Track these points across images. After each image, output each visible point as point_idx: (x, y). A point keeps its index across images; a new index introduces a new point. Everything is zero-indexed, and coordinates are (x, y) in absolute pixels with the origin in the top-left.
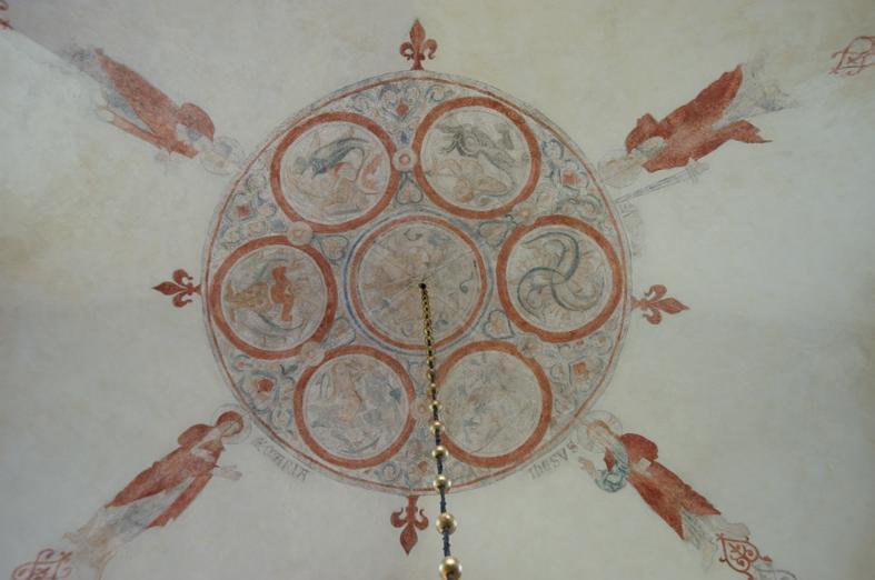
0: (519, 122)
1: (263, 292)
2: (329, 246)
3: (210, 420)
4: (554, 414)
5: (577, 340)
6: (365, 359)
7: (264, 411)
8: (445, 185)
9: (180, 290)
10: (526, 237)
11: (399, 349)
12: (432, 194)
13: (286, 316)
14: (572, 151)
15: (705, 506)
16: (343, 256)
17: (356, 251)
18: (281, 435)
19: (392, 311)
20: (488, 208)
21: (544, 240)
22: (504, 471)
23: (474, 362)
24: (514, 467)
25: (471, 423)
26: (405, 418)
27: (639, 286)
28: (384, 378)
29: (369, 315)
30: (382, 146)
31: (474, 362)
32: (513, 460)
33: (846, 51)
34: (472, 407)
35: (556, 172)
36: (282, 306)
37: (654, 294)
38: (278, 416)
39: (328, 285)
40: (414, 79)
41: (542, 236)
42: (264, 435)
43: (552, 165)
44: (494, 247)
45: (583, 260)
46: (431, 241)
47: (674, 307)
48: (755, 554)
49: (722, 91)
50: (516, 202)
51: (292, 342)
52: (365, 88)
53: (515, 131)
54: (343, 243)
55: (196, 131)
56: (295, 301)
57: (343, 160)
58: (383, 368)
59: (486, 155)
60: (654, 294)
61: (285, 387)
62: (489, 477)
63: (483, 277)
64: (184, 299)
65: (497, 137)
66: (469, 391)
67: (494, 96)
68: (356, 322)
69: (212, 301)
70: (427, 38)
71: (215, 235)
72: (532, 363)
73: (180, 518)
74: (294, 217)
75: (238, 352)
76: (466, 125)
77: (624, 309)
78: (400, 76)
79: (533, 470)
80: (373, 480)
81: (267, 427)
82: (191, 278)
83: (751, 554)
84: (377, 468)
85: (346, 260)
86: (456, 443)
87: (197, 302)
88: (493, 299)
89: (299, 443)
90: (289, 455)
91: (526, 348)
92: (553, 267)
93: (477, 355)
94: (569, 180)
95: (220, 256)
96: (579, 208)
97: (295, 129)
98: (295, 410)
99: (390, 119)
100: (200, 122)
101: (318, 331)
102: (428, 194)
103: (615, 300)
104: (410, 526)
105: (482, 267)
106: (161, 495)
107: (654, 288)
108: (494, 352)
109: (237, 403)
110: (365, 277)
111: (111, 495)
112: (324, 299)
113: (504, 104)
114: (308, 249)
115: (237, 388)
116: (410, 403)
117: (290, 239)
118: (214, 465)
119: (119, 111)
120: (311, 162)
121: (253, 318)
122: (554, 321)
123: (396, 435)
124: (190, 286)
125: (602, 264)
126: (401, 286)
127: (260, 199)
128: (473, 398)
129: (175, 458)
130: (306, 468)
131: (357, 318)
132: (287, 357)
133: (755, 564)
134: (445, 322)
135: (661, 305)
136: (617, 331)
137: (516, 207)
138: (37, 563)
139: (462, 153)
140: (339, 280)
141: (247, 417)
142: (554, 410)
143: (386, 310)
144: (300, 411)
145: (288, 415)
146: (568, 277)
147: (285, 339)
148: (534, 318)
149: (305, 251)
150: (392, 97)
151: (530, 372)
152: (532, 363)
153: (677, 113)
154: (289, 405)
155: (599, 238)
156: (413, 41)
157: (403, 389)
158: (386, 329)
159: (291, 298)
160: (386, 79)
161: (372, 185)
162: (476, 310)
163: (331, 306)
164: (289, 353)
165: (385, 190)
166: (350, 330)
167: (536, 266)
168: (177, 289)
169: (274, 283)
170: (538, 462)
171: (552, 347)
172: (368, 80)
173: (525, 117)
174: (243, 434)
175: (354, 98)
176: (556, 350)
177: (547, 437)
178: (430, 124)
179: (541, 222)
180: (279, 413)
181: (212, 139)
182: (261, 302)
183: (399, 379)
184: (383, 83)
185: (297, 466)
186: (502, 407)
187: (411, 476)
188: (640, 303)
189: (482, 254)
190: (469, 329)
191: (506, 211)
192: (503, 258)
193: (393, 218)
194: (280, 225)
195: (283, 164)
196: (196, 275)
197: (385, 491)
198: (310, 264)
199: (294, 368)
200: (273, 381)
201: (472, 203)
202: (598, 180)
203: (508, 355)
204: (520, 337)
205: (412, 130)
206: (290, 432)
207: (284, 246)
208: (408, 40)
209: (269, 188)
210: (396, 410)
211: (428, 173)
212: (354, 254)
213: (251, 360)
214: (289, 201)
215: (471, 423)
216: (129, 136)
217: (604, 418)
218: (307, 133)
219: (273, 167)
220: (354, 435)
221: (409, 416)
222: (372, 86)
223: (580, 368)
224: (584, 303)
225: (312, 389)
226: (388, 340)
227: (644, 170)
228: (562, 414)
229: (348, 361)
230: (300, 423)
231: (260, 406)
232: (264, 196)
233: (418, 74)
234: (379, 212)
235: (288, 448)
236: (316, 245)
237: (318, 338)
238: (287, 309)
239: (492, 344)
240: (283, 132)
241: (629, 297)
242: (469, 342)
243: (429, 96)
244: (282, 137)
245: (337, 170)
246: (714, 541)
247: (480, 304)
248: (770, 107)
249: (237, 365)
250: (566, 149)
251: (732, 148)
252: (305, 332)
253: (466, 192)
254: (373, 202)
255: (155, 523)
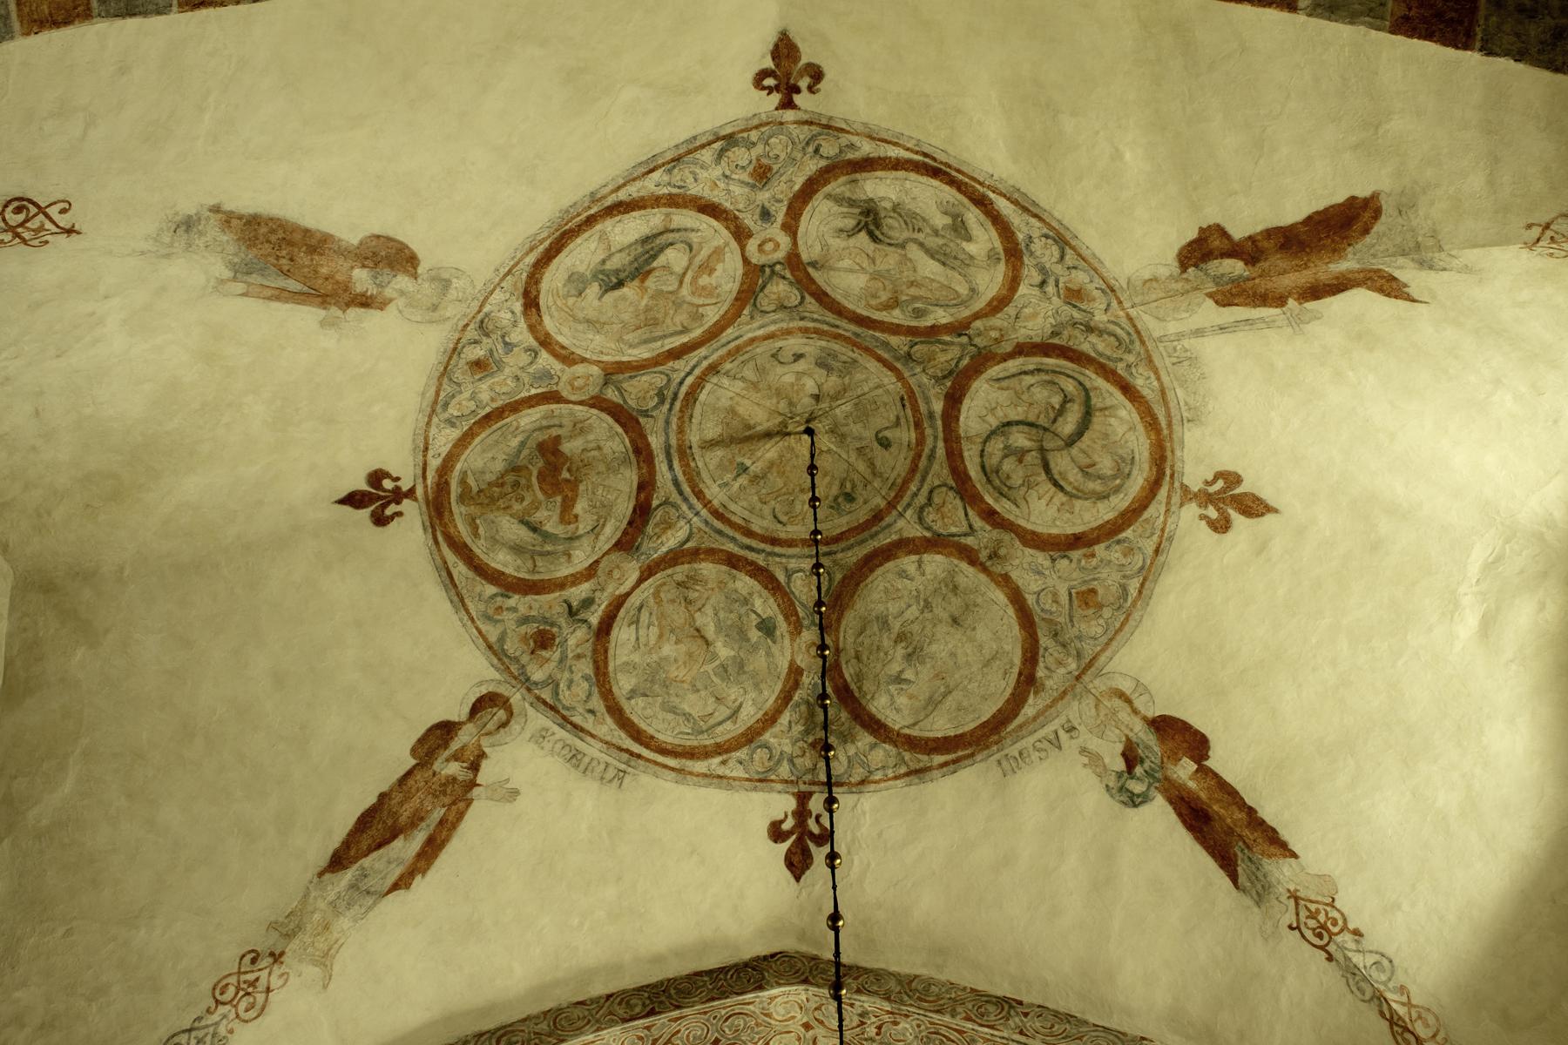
0: (981, 202)
1: (523, 481)
2: (637, 390)
3: (458, 713)
4: (1041, 673)
5: (1084, 551)
6: (708, 569)
7: (545, 684)
8: (850, 280)
9: (379, 498)
10: (995, 371)
11: (768, 548)
12: (822, 297)
13: (567, 515)
14: (1079, 255)
15: (1276, 843)
16: (662, 402)
17: (684, 389)
18: (577, 720)
19: (755, 479)
20: (927, 322)
21: (1029, 380)
22: (954, 762)
23: (903, 574)
24: (972, 755)
25: (898, 679)
26: (786, 665)
27: (1194, 470)
28: (746, 601)
29: (714, 492)
30: (725, 232)
31: (903, 574)
32: (970, 744)
33: (1547, 227)
34: (900, 651)
35: (1051, 281)
36: (559, 499)
37: (1220, 484)
38: (569, 688)
39: (637, 451)
40: (781, 124)
41: (1025, 373)
42: (548, 723)
43: (1042, 270)
44: (939, 380)
45: (1097, 419)
46: (821, 364)
47: (1254, 507)
48: (1340, 922)
49: (1345, 222)
50: (977, 316)
51: (581, 558)
52: (690, 152)
53: (973, 216)
54: (660, 381)
55: (387, 271)
56: (582, 487)
57: (655, 264)
58: (745, 583)
59: (921, 245)
60: (1220, 484)
61: (576, 638)
62: (929, 769)
63: (918, 425)
64: (389, 511)
65: (941, 221)
66: (896, 626)
67: (934, 159)
68: (691, 507)
69: (437, 508)
70: (804, 60)
71: (433, 411)
72: (1005, 581)
73: (430, 874)
74: (568, 359)
75: (491, 590)
76: (883, 199)
77: (1168, 503)
78: (756, 122)
79: (1004, 763)
80: (734, 774)
81: (552, 708)
82: (398, 479)
83: (1335, 923)
84: (742, 754)
85: (667, 406)
86: (874, 710)
87: (412, 513)
88: (936, 467)
89: (607, 728)
90: (592, 750)
91: (994, 555)
92: (1042, 421)
93: (908, 562)
94: (1074, 296)
95: (444, 439)
96: (1093, 338)
97: (564, 234)
98: (597, 675)
99: (737, 190)
100: (394, 257)
101: (625, 533)
102: (812, 294)
103: (1154, 486)
104: (800, 840)
105: (915, 409)
106: (398, 843)
107: (1219, 475)
108: (939, 558)
109: (497, 676)
110: (704, 427)
111: (324, 860)
112: (628, 479)
113: (954, 173)
114: (597, 403)
115: (495, 651)
116: (793, 640)
117: (564, 394)
118: (473, 784)
119: (255, 279)
120: (595, 276)
121: (510, 529)
122: (1043, 512)
123: (770, 697)
124: (397, 490)
125: (1132, 428)
126: (768, 435)
127: (506, 344)
128: (901, 637)
129: (411, 782)
130: (623, 767)
131: (693, 500)
132: (574, 584)
133: (1339, 939)
134: (850, 498)
135: (1232, 501)
136: (1155, 538)
137: (978, 324)
138: (239, 973)
139: (874, 239)
140: (655, 442)
141: (517, 698)
142: (1041, 665)
143: (743, 480)
144: (606, 674)
145: (586, 685)
146: (1070, 442)
147: (569, 556)
148: (1008, 505)
149: (593, 406)
150: (740, 155)
151: (1000, 596)
152: (1005, 581)
153: (1269, 233)
154: (586, 667)
155: (1127, 389)
156: (777, 66)
157: (780, 618)
158: (746, 514)
159: (574, 484)
160: (728, 130)
161: (709, 291)
162: (906, 482)
163: (646, 486)
164: (575, 579)
165: (734, 294)
166: (682, 523)
167: (1013, 416)
168: (375, 499)
169: (541, 464)
170: (1013, 751)
171: (1042, 558)
172: (695, 138)
173: (992, 195)
174: (515, 726)
175: (670, 171)
176: (1047, 563)
177: (1029, 710)
178: (815, 192)
179: (1021, 350)
180: (571, 682)
181: (415, 276)
182: (523, 499)
183: (772, 600)
184: (724, 138)
185: (607, 765)
186: (953, 655)
187: (798, 761)
188: (1196, 495)
189: (916, 389)
190: (894, 513)
191: (959, 328)
192: (954, 400)
193: (750, 335)
194: (547, 375)
195: (544, 286)
196: (404, 469)
197: (755, 789)
198: (602, 423)
199: (588, 603)
200: (555, 630)
201: (896, 312)
202: (1127, 304)
203: (964, 565)
204: (984, 537)
205: (779, 201)
206: (591, 712)
207: (554, 406)
208: (769, 63)
209: (522, 324)
210: (769, 654)
211: (814, 264)
212: (681, 396)
213: (514, 600)
214: (560, 339)
215: (898, 679)
216: (275, 305)
217: (1126, 686)
218: (586, 235)
219: (526, 294)
220: (694, 704)
221: (792, 663)
222: (703, 146)
223: (1087, 598)
224: (1095, 486)
225: (622, 634)
226: (749, 533)
227: (1210, 303)
228: (1053, 673)
229: (679, 577)
230: (607, 695)
231: (538, 675)
232: (514, 337)
233: (789, 115)
234: (723, 329)
235: (589, 739)
236: (611, 394)
237: (626, 543)
238: (568, 505)
239: (937, 543)
240: (541, 242)
241: (1177, 484)
242: (895, 537)
243: (811, 149)
244: (541, 248)
245: (643, 281)
246: (1283, 899)
247: (913, 469)
248: (1426, 265)
249: (491, 612)
250: (1069, 251)
251: (1359, 300)
252: (602, 538)
253: (884, 297)
254: (712, 315)
255: (395, 887)
